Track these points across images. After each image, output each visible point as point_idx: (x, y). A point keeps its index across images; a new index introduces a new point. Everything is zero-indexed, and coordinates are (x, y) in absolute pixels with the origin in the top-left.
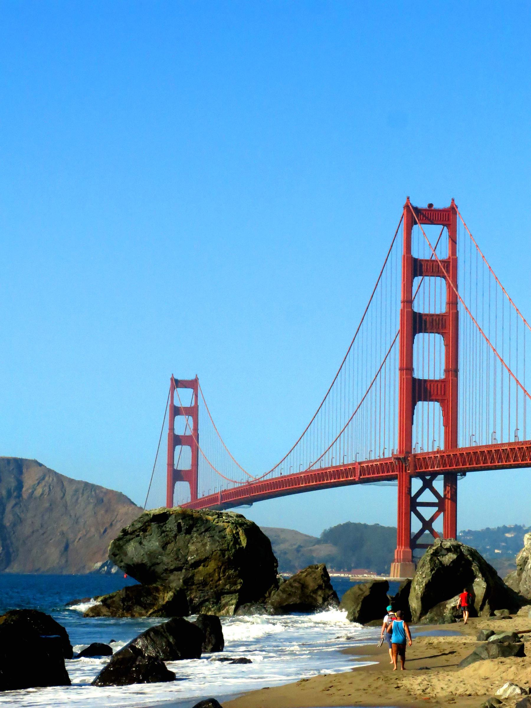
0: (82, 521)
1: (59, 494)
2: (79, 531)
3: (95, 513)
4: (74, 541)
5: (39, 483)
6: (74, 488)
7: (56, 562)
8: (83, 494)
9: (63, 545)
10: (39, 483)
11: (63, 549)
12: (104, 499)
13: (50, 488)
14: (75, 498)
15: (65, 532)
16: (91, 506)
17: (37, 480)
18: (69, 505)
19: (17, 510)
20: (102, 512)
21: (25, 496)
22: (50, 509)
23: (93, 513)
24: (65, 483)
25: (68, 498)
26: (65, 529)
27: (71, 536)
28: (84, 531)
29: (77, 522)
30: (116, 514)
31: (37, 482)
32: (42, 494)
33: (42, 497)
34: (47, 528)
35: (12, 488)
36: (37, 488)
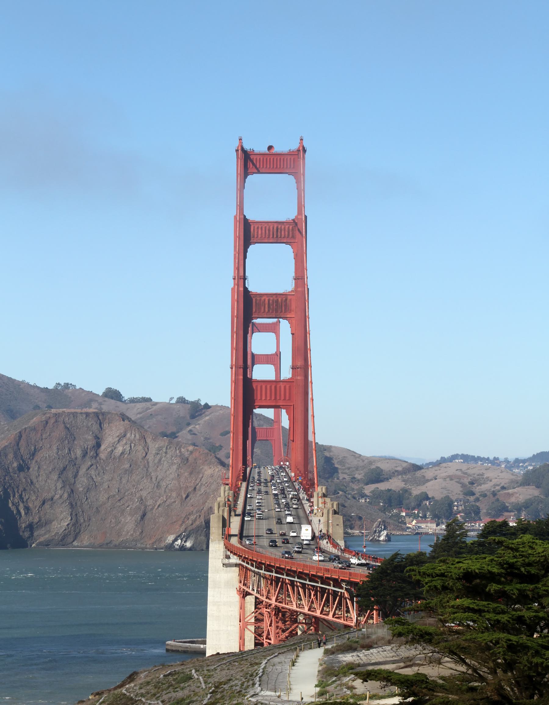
0: (163, 484)
1: (141, 454)
2: (159, 498)
3: (178, 475)
4: (152, 509)
5: (119, 441)
6: (157, 446)
7: (129, 534)
8: (166, 453)
9: (140, 513)
10: (119, 441)
11: (139, 518)
12: (190, 459)
13: (131, 446)
14: (158, 457)
15: (143, 498)
16: (175, 467)
17: (118, 436)
18: (150, 465)
19: (93, 472)
20: (186, 474)
21: (103, 456)
22: (129, 472)
23: (176, 475)
24: (148, 440)
25: (150, 457)
26: (144, 494)
27: (150, 502)
28: (165, 497)
29: (158, 486)
30: (201, 476)
31: (117, 439)
32: (122, 453)
33: (122, 456)
34: (125, 493)
35: (89, 447)
36: (118, 446)
